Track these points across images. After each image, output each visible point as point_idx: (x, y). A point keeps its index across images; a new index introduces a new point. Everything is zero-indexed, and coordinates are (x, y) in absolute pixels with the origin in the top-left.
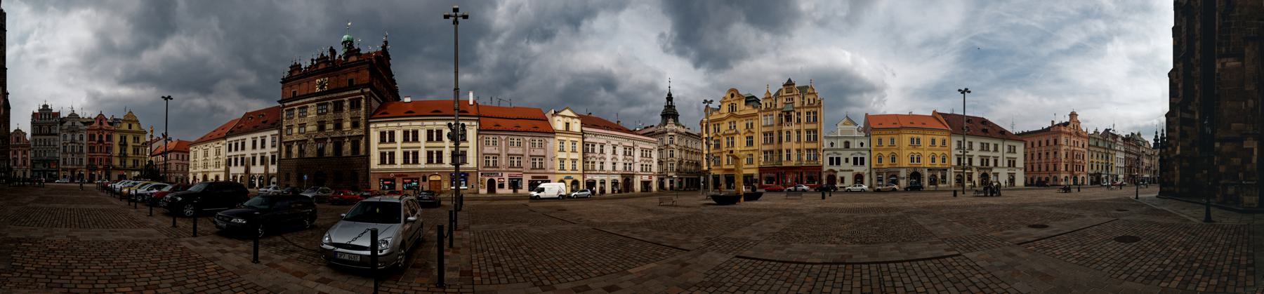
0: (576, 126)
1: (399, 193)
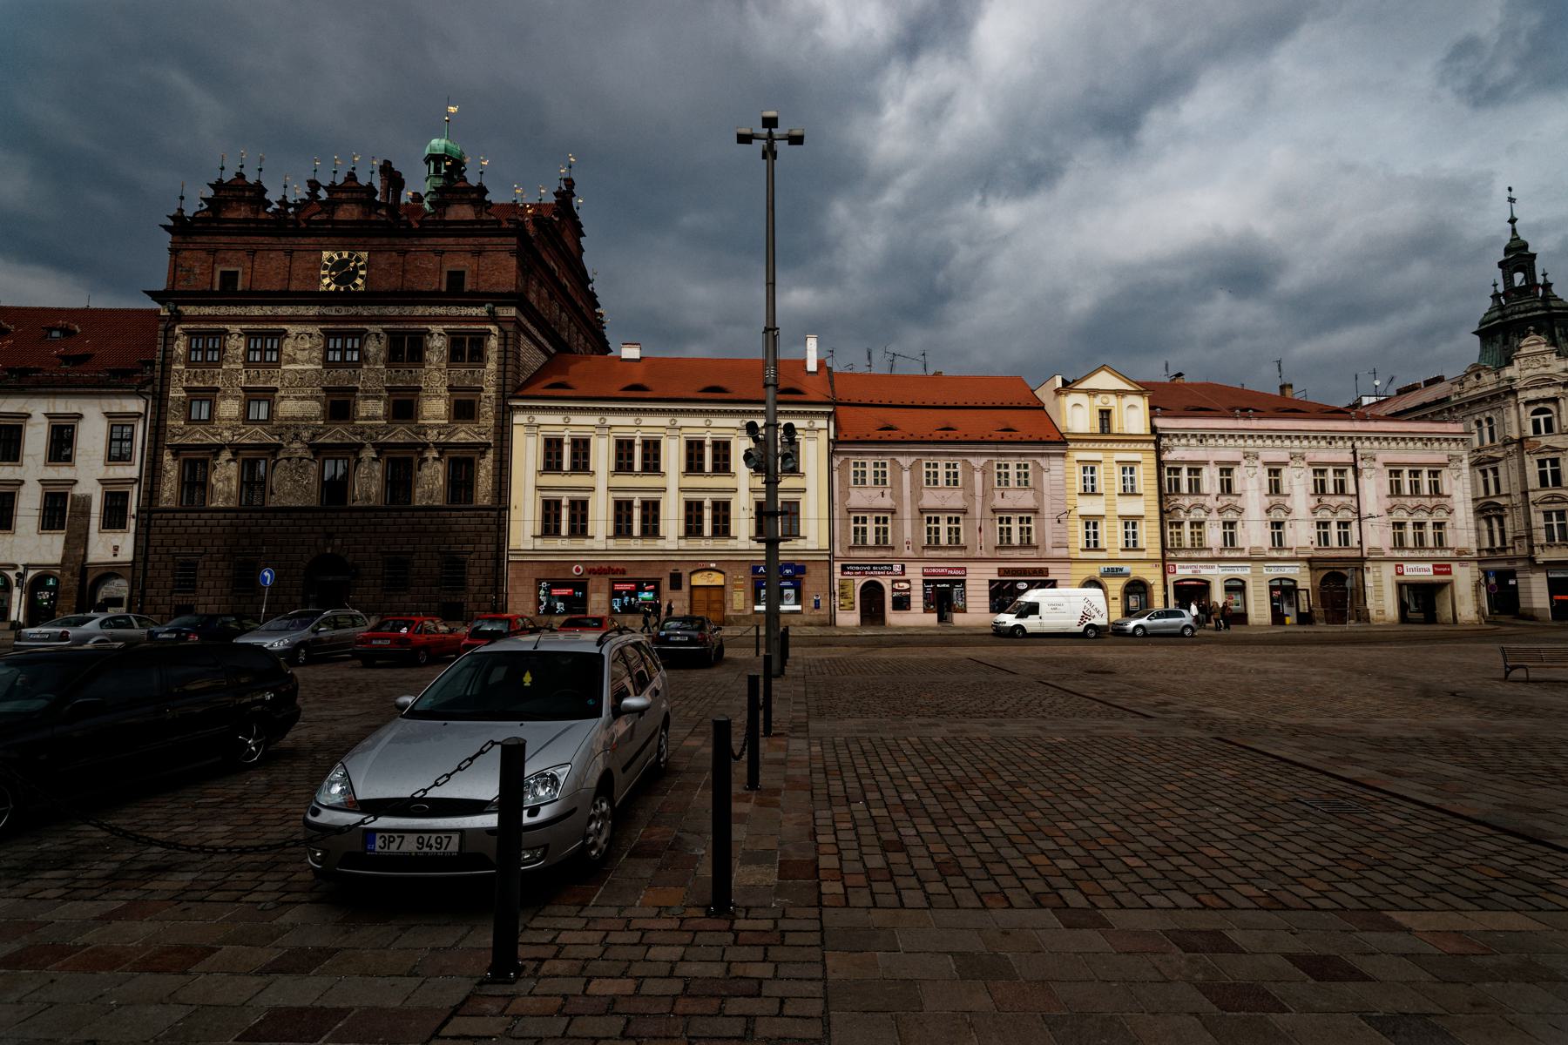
0: (1133, 416)
1: (599, 623)
